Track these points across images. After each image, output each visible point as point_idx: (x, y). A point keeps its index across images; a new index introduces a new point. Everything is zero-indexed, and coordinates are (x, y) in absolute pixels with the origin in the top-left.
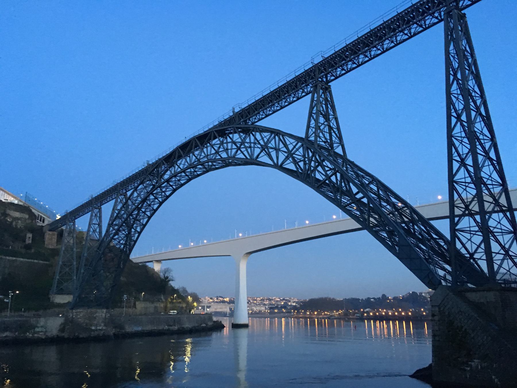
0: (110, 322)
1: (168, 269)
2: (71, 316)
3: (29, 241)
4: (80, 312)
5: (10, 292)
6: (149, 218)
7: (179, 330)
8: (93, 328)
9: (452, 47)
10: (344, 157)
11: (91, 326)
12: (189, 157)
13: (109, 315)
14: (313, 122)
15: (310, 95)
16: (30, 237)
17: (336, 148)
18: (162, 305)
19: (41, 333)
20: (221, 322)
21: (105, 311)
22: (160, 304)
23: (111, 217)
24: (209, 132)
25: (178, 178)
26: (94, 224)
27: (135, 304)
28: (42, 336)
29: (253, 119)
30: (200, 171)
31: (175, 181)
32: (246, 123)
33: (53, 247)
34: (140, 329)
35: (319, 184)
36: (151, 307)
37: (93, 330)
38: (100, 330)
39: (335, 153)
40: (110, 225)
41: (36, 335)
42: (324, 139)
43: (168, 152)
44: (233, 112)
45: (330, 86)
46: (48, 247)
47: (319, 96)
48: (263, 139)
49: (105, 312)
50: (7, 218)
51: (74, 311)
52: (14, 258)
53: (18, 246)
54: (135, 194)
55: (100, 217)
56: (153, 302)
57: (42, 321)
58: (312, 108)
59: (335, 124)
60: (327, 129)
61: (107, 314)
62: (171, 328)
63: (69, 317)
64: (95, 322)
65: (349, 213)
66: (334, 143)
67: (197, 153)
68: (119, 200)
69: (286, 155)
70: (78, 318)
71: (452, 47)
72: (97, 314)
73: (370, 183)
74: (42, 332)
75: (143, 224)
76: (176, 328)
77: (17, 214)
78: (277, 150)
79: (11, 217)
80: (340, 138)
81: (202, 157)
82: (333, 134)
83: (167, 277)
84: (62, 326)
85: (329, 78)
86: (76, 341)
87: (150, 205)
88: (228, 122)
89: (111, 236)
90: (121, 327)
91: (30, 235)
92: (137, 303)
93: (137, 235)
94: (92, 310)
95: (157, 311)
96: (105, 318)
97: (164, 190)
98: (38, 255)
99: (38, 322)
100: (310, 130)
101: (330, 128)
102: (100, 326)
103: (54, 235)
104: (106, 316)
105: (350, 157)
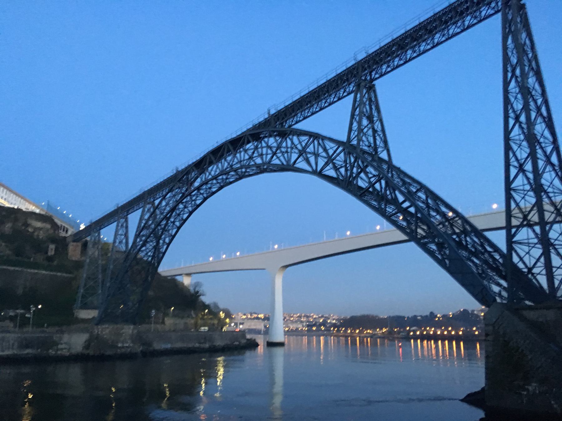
0: (138, 338)
2: (97, 332)
3: (51, 253)
4: (106, 328)
6: (179, 228)
7: (210, 347)
8: (120, 345)
9: (510, 41)
10: (389, 163)
12: (221, 163)
14: (355, 125)
15: (352, 95)
16: (52, 249)
17: (380, 153)
18: (193, 321)
19: (64, 350)
20: (255, 340)
21: (132, 327)
23: (138, 227)
25: (209, 186)
27: (163, 319)
28: (66, 353)
29: (289, 122)
30: (232, 179)
31: (206, 188)
32: (282, 126)
33: (77, 259)
34: (169, 346)
35: (362, 192)
36: (181, 323)
38: (127, 347)
39: (380, 159)
40: (137, 236)
41: (59, 352)
42: (367, 143)
43: (198, 158)
44: (269, 113)
46: (71, 259)
47: (362, 97)
48: (300, 143)
51: (99, 327)
52: (36, 271)
53: (40, 258)
54: (164, 203)
55: (127, 227)
56: (182, 318)
57: (66, 338)
58: (354, 109)
59: (380, 126)
60: (370, 132)
62: (202, 346)
63: (94, 333)
64: (122, 339)
65: (395, 223)
67: (229, 158)
68: (146, 210)
69: (326, 160)
71: (510, 41)
73: (418, 190)
74: (65, 349)
75: (171, 235)
76: (207, 345)
77: (39, 224)
78: (317, 155)
79: (32, 227)
80: (385, 142)
81: (234, 163)
82: (378, 138)
83: (198, 292)
84: (87, 343)
85: (373, 76)
86: (102, 358)
87: (179, 215)
89: (138, 247)
90: (150, 344)
91: (52, 247)
92: (166, 319)
93: (165, 247)
94: (118, 326)
95: (186, 328)
97: (194, 198)
98: (60, 268)
99: (61, 339)
100: (352, 134)
101: (375, 131)
102: (127, 343)
103: (78, 246)
104: (133, 332)
105: (396, 162)
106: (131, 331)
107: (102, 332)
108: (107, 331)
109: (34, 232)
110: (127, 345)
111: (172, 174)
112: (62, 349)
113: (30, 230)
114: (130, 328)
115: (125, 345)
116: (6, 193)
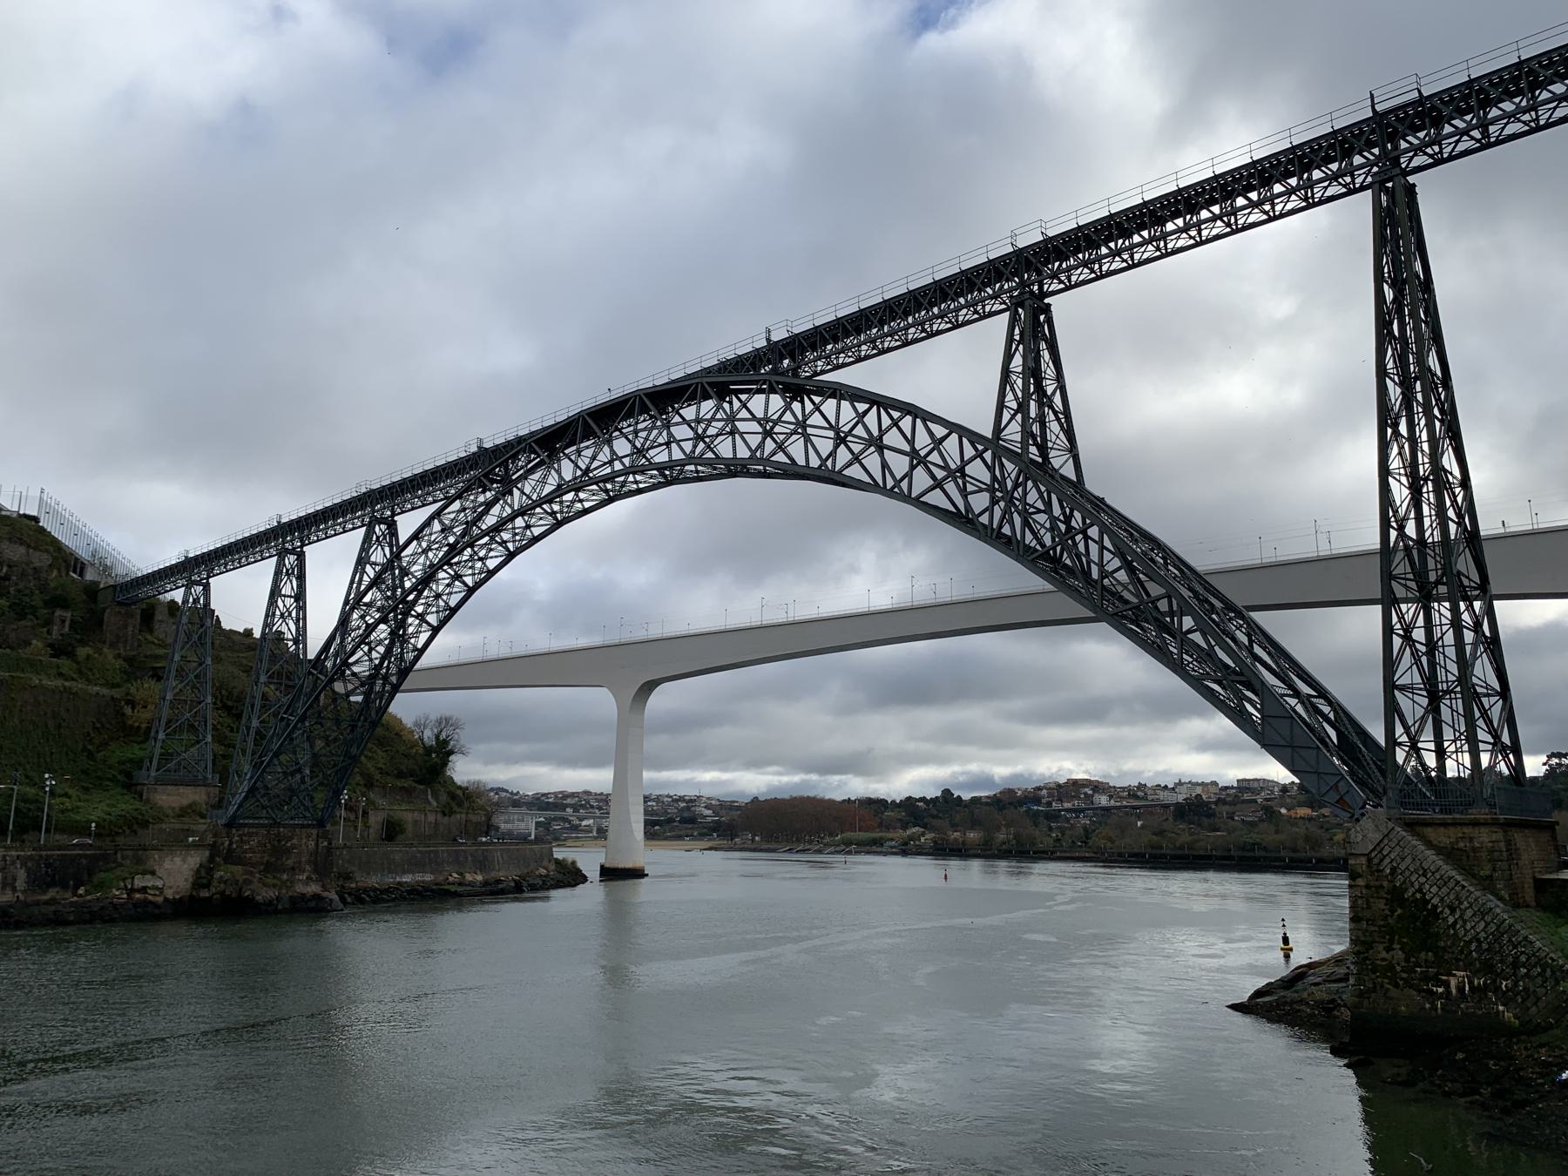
1: (447, 720)
2: (227, 843)
4: (250, 835)
5: (47, 776)
7: (486, 883)
13: (326, 844)
20: (574, 863)
24: (687, 383)
26: (285, 596)
44: (768, 340)
45: (1049, 305)
49: (314, 836)
61: (321, 840)
64: (290, 862)
66: (1051, 449)
70: (245, 852)
72: (295, 841)
83: (446, 742)
85: (1046, 287)
88: (748, 364)
96: (316, 852)
102: (304, 871)
104: (317, 845)
105: (1092, 485)
106: (312, 844)
111: (463, 454)
112: (144, 890)
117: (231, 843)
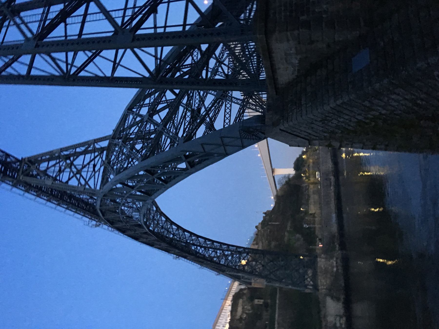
4: (321, 281)
8: (335, 269)
10: (113, 138)
11: (333, 271)
18: (311, 186)
21: (319, 259)
22: (311, 189)
28: (343, 320)
34: (334, 215)
36: (314, 198)
37: (337, 270)
38: (336, 263)
49: (320, 259)
50: (244, 318)
51: (320, 288)
52: (276, 322)
53: (266, 315)
56: (309, 196)
72: (322, 266)
76: (332, 178)
77: (240, 309)
79: (242, 314)
92: (310, 212)
94: (319, 271)
95: (318, 192)
96: (326, 258)
102: (333, 263)
104: (323, 258)
106: (323, 260)
107: (324, 285)
108: (323, 281)
109: (246, 313)
110: (335, 263)
113: (245, 316)
114: (320, 261)
115: (335, 264)
116: (219, 326)
117: (324, 289)
